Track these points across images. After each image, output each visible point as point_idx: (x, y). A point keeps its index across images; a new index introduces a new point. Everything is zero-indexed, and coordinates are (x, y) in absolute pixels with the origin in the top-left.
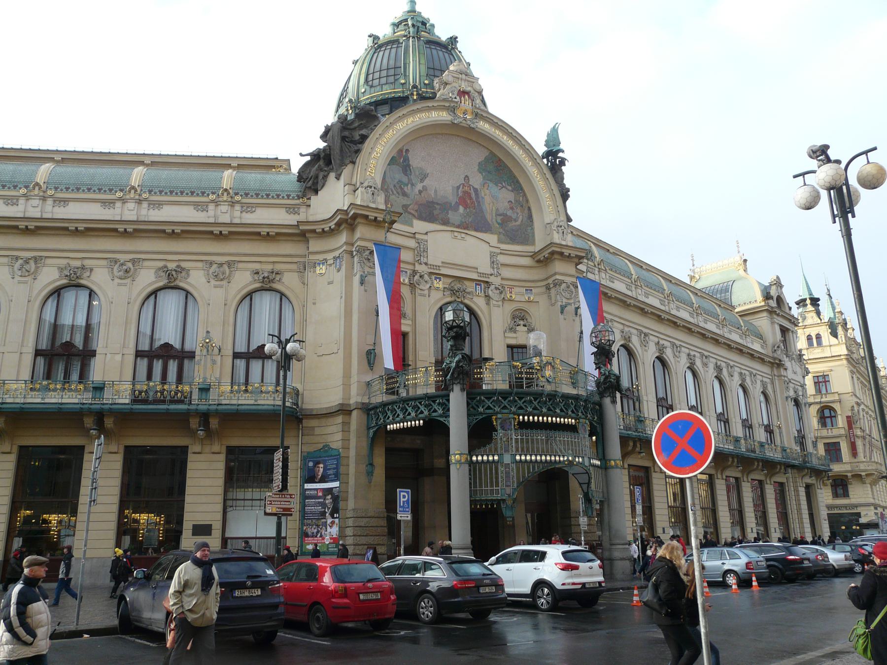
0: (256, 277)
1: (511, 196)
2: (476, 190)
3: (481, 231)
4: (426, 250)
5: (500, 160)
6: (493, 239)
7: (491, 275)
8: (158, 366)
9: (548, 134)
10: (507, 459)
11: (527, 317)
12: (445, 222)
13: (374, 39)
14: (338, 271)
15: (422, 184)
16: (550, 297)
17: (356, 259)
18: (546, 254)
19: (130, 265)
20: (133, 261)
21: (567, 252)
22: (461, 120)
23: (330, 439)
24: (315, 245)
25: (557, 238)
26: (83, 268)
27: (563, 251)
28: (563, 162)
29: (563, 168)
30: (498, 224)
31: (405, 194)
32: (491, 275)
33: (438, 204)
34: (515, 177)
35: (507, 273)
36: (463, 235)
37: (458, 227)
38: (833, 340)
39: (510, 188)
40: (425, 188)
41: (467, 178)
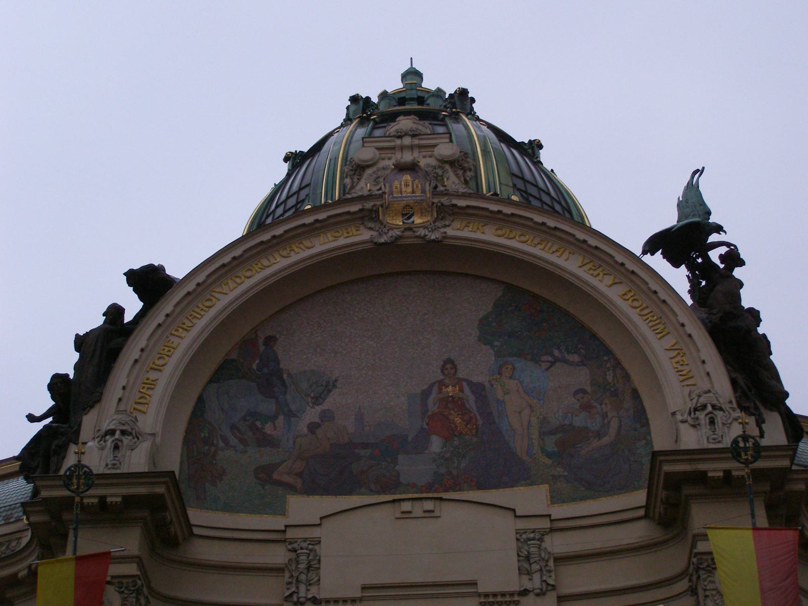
1: (581, 377)
2: (478, 389)
3: (496, 487)
4: (313, 566)
5: (535, 296)
6: (532, 499)
7: (525, 593)
9: (680, 205)
12: (389, 484)
13: (295, 159)
15: (319, 409)
18: (662, 494)
21: (715, 469)
22: (398, 232)
25: (691, 439)
27: (702, 467)
28: (733, 259)
29: (738, 273)
30: (549, 455)
31: (266, 441)
32: (525, 593)
33: (365, 446)
34: (583, 327)
36: (429, 505)
37: (429, 488)
39: (575, 358)
40: (327, 416)
41: (449, 365)
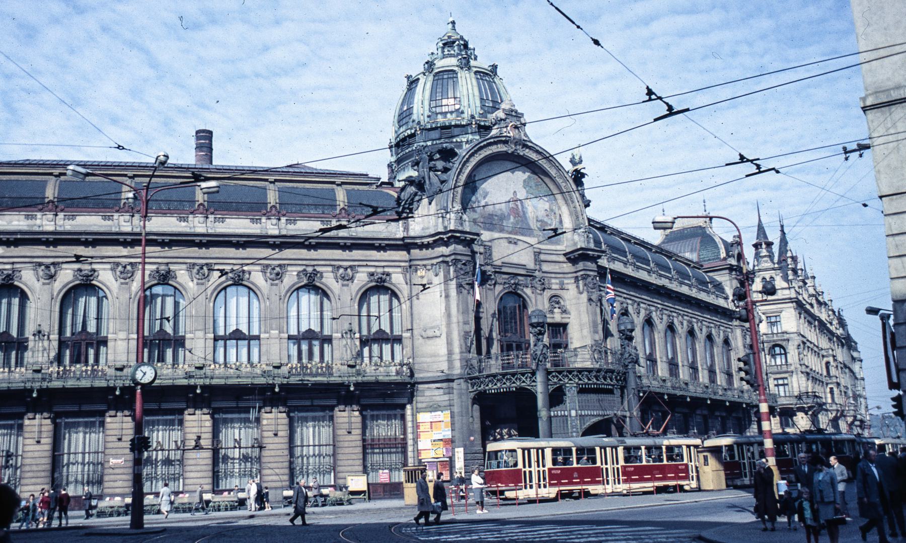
0: (372, 278)
3: (525, 235)
8: (305, 347)
10: (573, 413)
11: (561, 301)
12: (502, 231)
14: (436, 275)
16: (578, 287)
17: (452, 269)
19: (278, 269)
20: (280, 266)
23: (438, 398)
24: (415, 252)
26: (244, 272)
28: (583, 175)
35: (545, 267)
38: (785, 285)
